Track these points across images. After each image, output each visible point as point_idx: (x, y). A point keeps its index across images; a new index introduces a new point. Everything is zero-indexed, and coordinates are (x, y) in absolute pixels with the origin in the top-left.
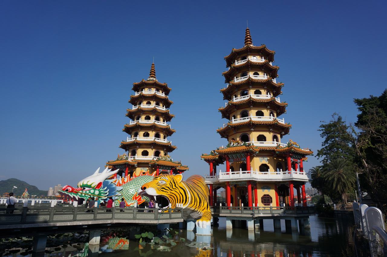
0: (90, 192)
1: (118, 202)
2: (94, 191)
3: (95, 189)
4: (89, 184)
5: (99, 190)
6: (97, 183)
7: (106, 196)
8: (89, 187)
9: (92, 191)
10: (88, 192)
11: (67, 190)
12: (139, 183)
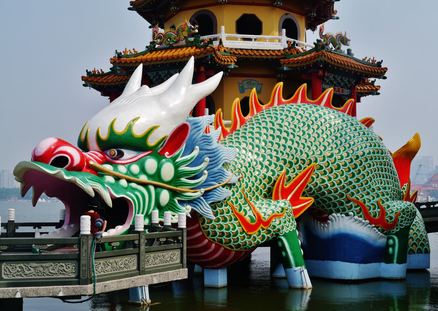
0: (143, 170)
1: (228, 212)
2: (159, 162)
3: (158, 152)
4: (138, 131)
6: (166, 131)
7: (199, 188)
8: (139, 145)
9: (151, 164)
10: (135, 168)
11: (61, 162)
12: (285, 135)
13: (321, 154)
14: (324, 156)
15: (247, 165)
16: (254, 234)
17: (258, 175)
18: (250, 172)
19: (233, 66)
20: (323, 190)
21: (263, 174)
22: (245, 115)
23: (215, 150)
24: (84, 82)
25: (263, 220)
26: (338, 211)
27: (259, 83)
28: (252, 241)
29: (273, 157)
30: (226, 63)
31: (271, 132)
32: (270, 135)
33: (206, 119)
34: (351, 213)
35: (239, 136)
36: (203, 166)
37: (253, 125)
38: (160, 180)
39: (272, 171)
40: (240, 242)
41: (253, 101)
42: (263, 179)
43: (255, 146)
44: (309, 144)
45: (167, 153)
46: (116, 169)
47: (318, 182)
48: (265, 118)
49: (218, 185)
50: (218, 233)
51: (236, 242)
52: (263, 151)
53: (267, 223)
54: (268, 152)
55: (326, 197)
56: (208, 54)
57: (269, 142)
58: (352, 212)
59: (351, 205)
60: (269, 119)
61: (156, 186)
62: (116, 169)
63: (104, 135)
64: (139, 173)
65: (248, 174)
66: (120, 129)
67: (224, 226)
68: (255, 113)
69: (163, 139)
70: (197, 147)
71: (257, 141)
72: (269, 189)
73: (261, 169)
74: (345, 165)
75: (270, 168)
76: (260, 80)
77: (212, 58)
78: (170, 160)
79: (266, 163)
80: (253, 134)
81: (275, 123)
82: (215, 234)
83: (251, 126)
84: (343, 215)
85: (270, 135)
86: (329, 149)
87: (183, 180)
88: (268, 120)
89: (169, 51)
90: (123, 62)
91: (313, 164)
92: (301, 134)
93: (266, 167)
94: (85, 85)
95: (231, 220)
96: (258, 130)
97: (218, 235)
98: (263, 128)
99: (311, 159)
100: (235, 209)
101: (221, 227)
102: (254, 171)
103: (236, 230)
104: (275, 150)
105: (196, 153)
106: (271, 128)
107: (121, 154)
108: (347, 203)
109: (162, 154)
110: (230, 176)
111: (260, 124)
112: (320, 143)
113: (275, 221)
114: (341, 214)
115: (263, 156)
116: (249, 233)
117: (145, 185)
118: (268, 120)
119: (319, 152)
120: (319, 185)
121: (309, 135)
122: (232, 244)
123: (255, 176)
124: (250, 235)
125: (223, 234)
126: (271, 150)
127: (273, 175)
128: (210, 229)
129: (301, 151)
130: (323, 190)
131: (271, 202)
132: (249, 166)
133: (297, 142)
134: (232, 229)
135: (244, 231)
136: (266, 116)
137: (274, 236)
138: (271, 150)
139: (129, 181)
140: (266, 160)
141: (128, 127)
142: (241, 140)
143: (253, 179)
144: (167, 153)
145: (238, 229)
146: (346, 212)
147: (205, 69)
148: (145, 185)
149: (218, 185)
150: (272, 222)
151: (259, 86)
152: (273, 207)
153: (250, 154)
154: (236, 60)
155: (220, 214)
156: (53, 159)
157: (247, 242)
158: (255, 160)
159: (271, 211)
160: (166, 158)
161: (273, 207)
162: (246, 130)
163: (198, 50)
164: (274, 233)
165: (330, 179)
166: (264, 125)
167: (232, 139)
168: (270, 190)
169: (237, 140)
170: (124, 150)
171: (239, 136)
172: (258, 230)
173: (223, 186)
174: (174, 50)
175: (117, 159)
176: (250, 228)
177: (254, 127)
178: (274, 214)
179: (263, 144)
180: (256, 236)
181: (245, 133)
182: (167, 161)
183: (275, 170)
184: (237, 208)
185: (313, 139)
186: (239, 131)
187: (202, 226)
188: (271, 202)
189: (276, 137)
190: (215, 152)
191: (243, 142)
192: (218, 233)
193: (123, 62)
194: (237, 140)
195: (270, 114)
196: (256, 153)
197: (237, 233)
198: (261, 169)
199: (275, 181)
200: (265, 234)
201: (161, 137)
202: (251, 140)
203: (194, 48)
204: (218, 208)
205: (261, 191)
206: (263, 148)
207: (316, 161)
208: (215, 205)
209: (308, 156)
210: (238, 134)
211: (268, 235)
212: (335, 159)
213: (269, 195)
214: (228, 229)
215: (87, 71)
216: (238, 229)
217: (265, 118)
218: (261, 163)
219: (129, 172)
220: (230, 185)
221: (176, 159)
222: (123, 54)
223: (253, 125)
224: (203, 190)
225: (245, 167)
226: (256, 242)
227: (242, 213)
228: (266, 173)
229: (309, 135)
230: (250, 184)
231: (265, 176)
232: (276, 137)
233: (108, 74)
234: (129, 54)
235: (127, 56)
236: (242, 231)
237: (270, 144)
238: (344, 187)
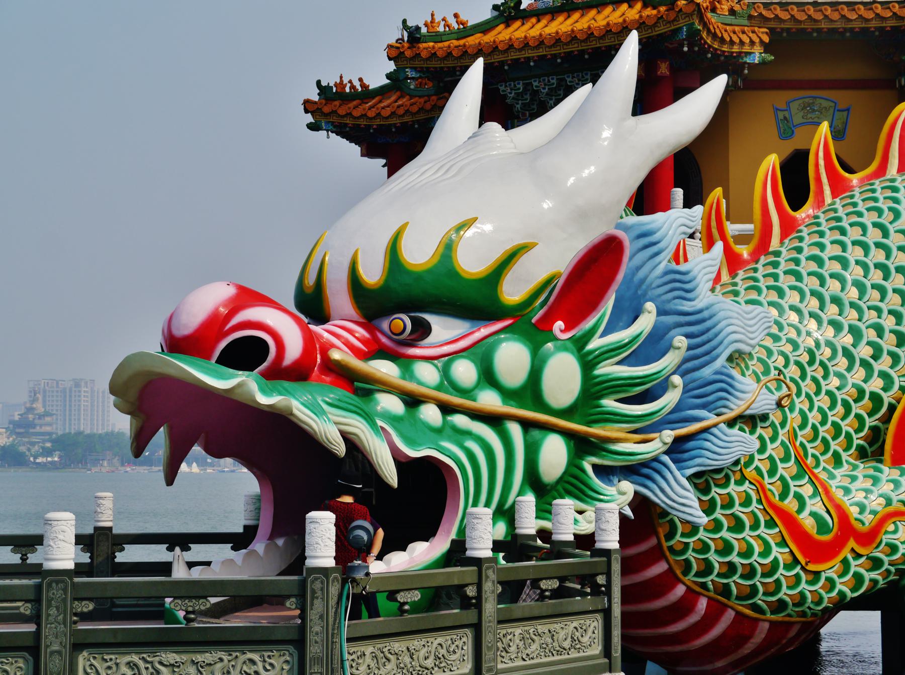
0: (488, 377)
1: (747, 502)
3: (533, 323)
4: (473, 262)
5: (580, 344)
6: (555, 258)
7: (656, 427)
8: (476, 302)
9: (512, 357)
10: (465, 371)
11: (247, 354)
15: (805, 358)
16: (830, 569)
17: (838, 389)
18: (814, 379)
19: (757, 56)
21: (854, 385)
22: (797, 205)
23: (706, 314)
24: (309, 118)
25: (858, 526)
27: (839, 107)
28: (822, 592)
29: (887, 335)
30: (736, 49)
31: (879, 256)
32: (877, 266)
33: (677, 220)
35: (779, 271)
36: (669, 361)
37: (821, 234)
38: (539, 403)
39: (884, 375)
40: (785, 593)
41: (822, 162)
42: (856, 401)
43: (828, 299)
45: (559, 325)
46: (407, 372)
48: (860, 215)
49: (713, 419)
50: (717, 565)
51: (772, 594)
52: (854, 314)
53: (869, 537)
54: (871, 316)
56: (682, 23)
57: (873, 287)
60: (873, 217)
61: (527, 425)
62: (407, 372)
63: (373, 274)
64: (478, 386)
65: (807, 386)
66: (419, 254)
67: (736, 544)
68: (828, 198)
69: (548, 282)
70: (650, 306)
71: (834, 286)
72: (875, 430)
73: (849, 369)
75: (877, 366)
76: (843, 97)
77: (694, 35)
78: (569, 344)
79: (864, 352)
80: (820, 262)
81: (891, 229)
82: (707, 568)
83: (816, 239)
85: (877, 266)
87: (609, 403)
88: (868, 219)
89: (561, 19)
90: (424, 55)
93: (864, 363)
94: (313, 127)
95: (755, 526)
96: (837, 251)
97: (716, 572)
98: (854, 243)
100: (769, 493)
101: (726, 549)
102: (825, 377)
103: (771, 558)
104: (890, 312)
105: (646, 323)
106: (878, 245)
107: (422, 330)
109: (545, 325)
110: (752, 394)
111: (843, 232)
113: (895, 531)
115: (855, 332)
116: (811, 567)
117: (494, 420)
118: (868, 219)
122: (759, 600)
123: (829, 393)
124: (817, 574)
125: (731, 568)
126: (878, 310)
127: (885, 389)
128: (690, 555)
131: (880, 471)
132: (811, 362)
134: (761, 555)
135: (796, 561)
136: (861, 208)
137: (891, 578)
138: (878, 310)
139: (447, 409)
140: (864, 341)
141: (441, 250)
142: (785, 282)
143: (823, 401)
144: (559, 325)
145: (778, 553)
147: (671, 68)
148: (494, 420)
149: (712, 419)
150: (886, 532)
151: (838, 115)
152: (887, 488)
153: (813, 325)
154: (766, 39)
155: (723, 507)
156: (223, 344)
157: (808, 595)
158: (829, 344)
159: (882, 501)
160: (556, 339)
161: (887, 488)
162: (799, 250)
163: (649, 12)
164: (892, 569)
166: (854, 234)
167: (755, 280)
168: (876, 436)
169: (771, 282)
170: (428, 317)
171: (779, 271)
172: (841, 557)
173: (731, 423)
174: (576, 16)
175: (411, 344)
176: (814, 550)
177: (825, 241)
178: (890, 509)
179: (854, 293)
180: (835, 576)
181: (797, 262)
182: (558, 349)
183: (892, 372)
184: (775, 490)
186: (777, 254)
187: (666, 545)
188: (880, 471)
189: (893, 271)
190: (703, 321)
191: (792, 288)
192: (717, 565)
193: (424, 55)
194: (771, 282)
195: (876, 200)
196: (832, 323)
197: (772, 569)
198: (849, 369)
199: (892, 408)
200: (862, 571)
201: (542, 276)
202: (814, 283)
203: (639, 6)
204: (714, 489)
205: (848, 436)
206: (852, 305)
208: (707, 481)
210: (775, 265)
211: (874, 575)
213: (872, 450)
214: (747, 553)
215: (319, 83)
216: (778, 553)
217: (860, 215)
218: (847, 353)
219: (448, 381)
220: (750, 421)
221: (586, 343)
222: (424, 30)
223: (821, 234)
224: (668, 435)
225: (797, 363)
226: (834, 594)
227: (790, 504)
228: (865, 381)
230: (814, 417)
231: (861, 392)
232: (893, 271)
233: (382, 91)
234: (441, 29)
235: (438, 37)
236: (789, 558)
237: (876, 294)
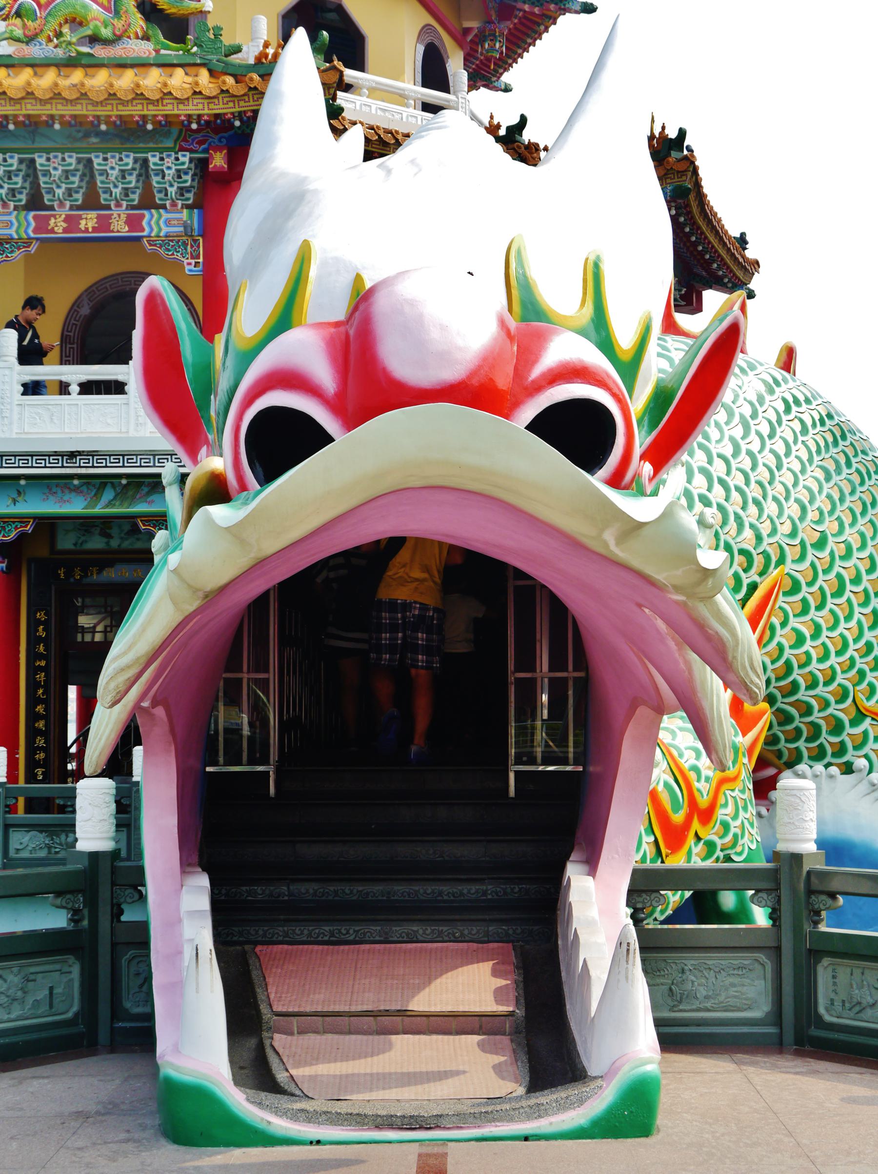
13: (793, 534)
14: (802, 543)
20: (796, 675)
26: (818, 755)
34: (862, 763)
44: (757, 493)
47: (784, 641)
55: (795, 704)
58: (866, 756)
59: (865, 733)
74: (856, 580)
84: (834, 770)
86: (812, 515)
91: (774, 573)
92: (728, 451)
99: (769, 550)
108: (854, 723)
112: (787, 491)
114: (827, 766)
119: (787, 528)
120: (788, 653)
121: (750, 453)
129: (738, 517)
130: (796, 675)
133: (721, 482)
146: (844, 759)
165: (817, 631)
185: (767, 475)
207: (781, 561)
209: (759, 538)
212: (832, 554)
229: (750, 453)
238: (852, 662)
